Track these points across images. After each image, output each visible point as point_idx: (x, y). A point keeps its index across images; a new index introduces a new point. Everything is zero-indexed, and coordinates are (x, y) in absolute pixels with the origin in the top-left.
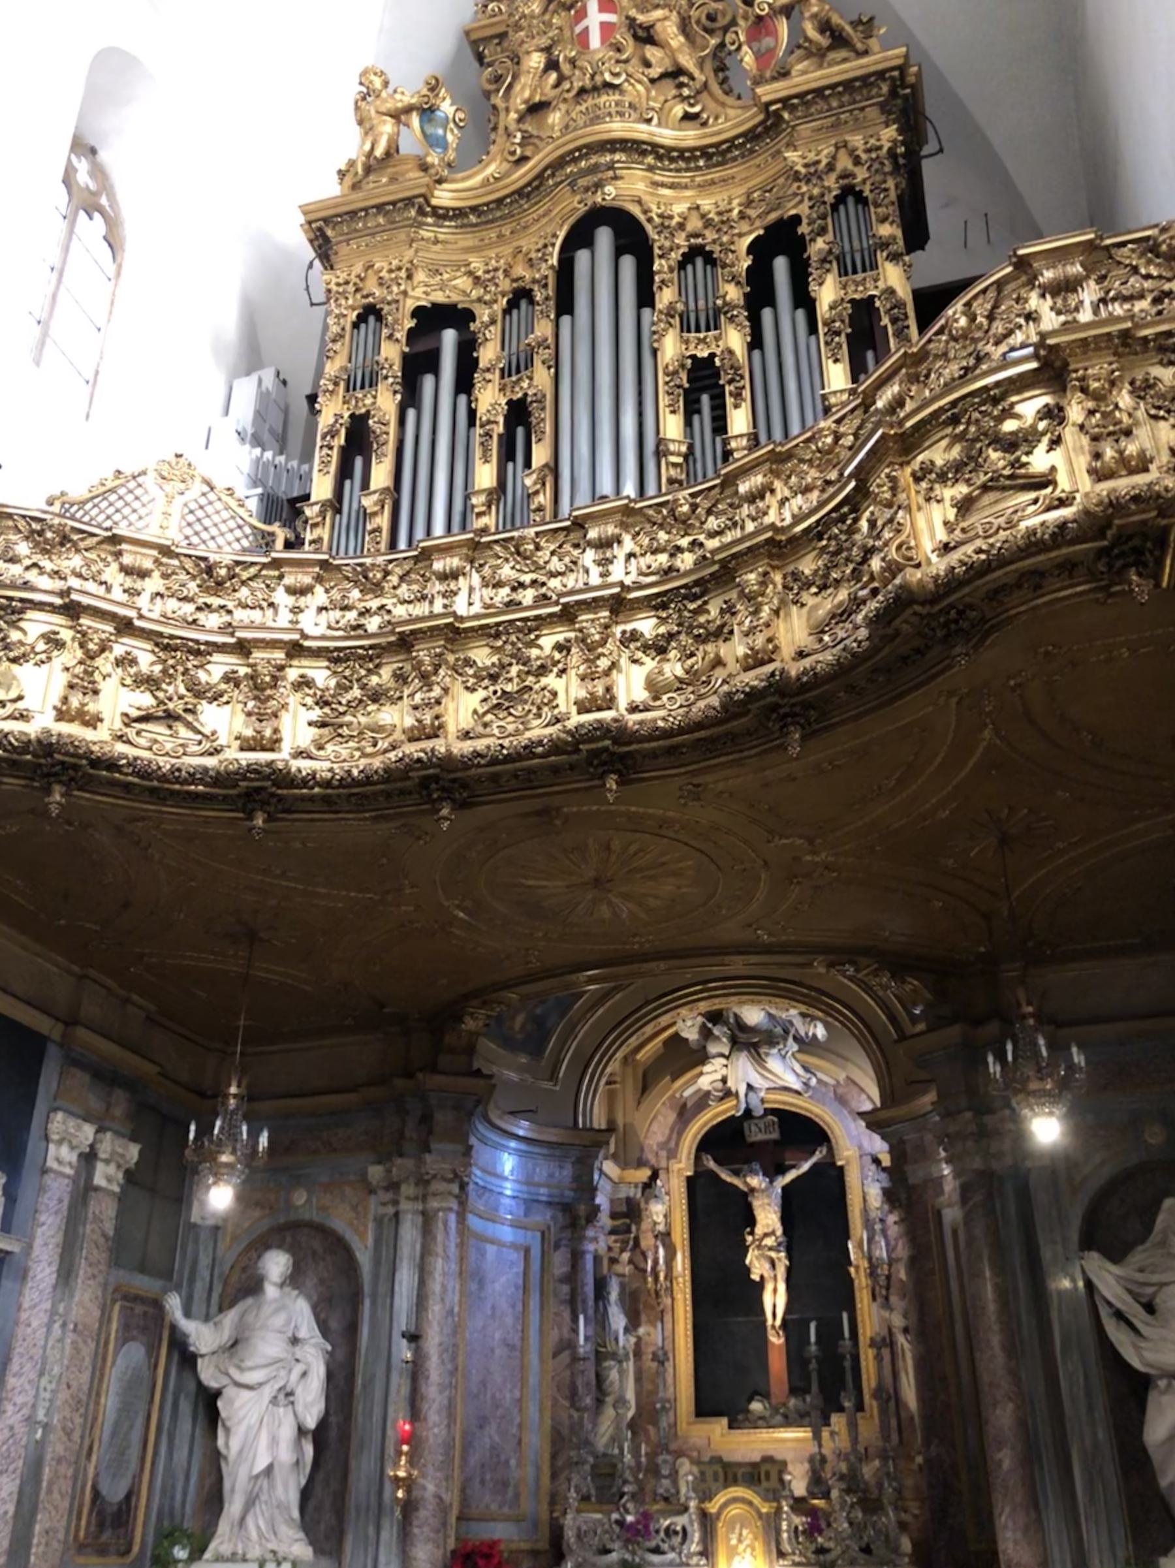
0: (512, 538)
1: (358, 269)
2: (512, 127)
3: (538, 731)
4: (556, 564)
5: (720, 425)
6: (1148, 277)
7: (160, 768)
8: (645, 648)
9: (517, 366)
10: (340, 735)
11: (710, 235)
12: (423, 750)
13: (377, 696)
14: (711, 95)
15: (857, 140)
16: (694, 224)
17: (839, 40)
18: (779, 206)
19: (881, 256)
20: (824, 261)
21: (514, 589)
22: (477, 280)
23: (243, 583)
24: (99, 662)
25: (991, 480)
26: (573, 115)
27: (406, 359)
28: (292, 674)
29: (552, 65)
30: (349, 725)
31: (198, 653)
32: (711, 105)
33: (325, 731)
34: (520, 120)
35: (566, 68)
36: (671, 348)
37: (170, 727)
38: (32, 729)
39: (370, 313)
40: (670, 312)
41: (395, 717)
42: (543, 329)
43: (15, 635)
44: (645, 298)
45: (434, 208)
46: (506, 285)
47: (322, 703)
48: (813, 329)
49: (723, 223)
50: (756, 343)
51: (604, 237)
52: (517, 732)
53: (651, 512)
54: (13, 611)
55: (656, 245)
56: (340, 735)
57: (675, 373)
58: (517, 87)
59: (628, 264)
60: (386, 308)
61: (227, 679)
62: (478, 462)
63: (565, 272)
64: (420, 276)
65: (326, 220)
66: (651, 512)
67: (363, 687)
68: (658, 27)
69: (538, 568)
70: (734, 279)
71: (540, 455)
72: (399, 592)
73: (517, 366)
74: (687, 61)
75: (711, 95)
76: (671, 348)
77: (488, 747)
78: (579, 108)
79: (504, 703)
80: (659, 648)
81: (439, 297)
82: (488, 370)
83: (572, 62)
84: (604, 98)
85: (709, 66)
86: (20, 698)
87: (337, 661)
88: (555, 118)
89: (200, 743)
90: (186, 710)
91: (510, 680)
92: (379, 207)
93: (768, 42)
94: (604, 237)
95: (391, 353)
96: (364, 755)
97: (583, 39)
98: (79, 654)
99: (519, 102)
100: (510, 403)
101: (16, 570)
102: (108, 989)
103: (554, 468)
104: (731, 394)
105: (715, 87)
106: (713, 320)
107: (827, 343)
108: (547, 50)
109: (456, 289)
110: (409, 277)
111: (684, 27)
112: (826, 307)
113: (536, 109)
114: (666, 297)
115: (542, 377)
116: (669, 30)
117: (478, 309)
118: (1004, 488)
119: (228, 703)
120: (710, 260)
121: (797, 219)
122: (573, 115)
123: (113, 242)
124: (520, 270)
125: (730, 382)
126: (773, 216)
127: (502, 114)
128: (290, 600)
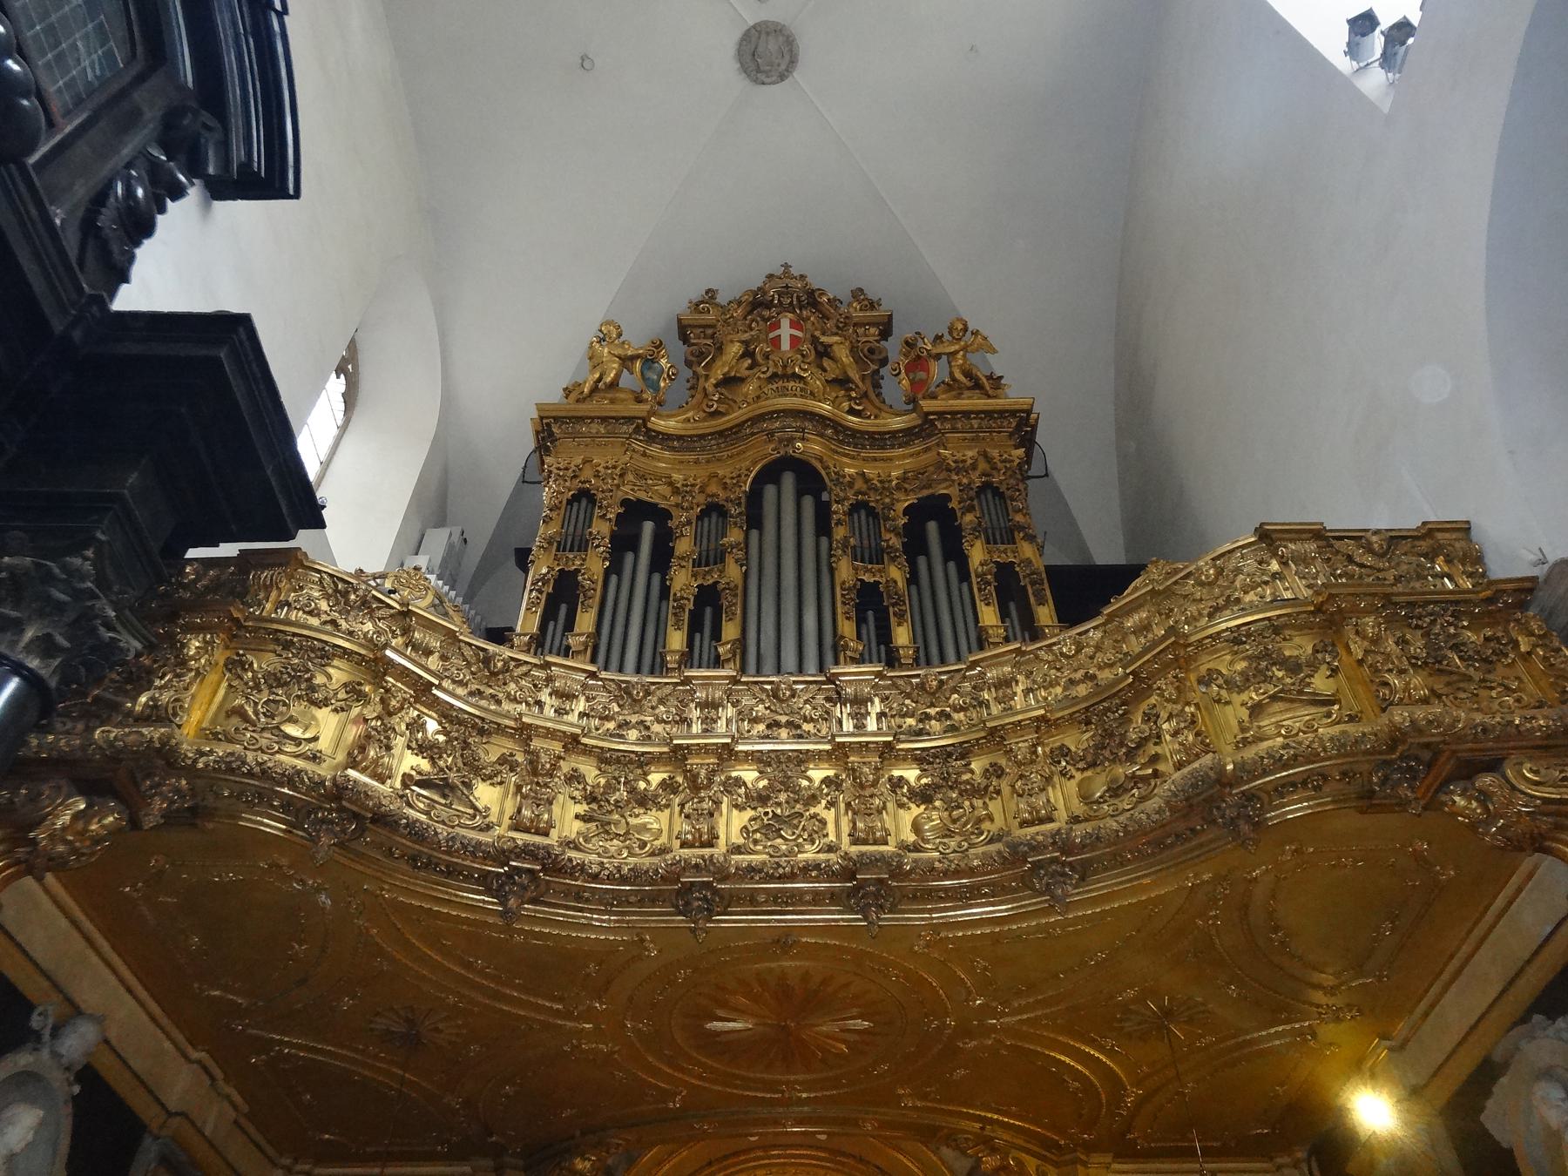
1: (578, 460)
2: (710, 389)
3: (809, 854)
5: (885, 636)
6: (1362, 566)
7: (436, 833)
10: (607, 832)
11: (873, 497)
12: (702, 857)
13: (644, 801)
14: (871, 402)
15: (995, 453)
16: (859, 484)
17: (977, 386)
18: (930, 486)
19: (1019, 536)
20: (974, 529)
21: (769, 727)
22: (676, 491)
23: (513, 679)
24: (395, 720)
25: (1281, 691)
27: (614, 537)
28: (565, 767)
29: (748, 354)
30: (616, 824)
31: (482, 732)
32: (870, 407)
33: (592, 825)
34: (716, 386)
35: (759, 358)
37: (444, 796)
38: (324, 771)
39: (585, 496)
40: (845, 544)
41: (658, 823)
42: (734, 536)
43: (319, 679)
45: (649, 430)
46: (701, 498)
47: (591, 798)
48: (964, 575)
49: (884, 487)
50: (913, 579)
51: (788, 480)
52: (790, 853)
54: (325, 654)
56: (607, 832)
57: (849, 589)
58: (719, 363)
60: (600, 496)
61: (503, 760)
62: (670, 629)
63: (754, 499)
64: (630, 477)
65: (556, 419)
66: (901, 682)
67: (632, 790)
68: (835, 348)
70: (894, 530)
71: (730, 631)
73: (711, 558)
74: (854, 375)
75: (871, 402)
77: (764, 863)
79: (771, 829)
80: (923, 796)
81: (643, 496)
82: (683, 558)
83: (767, 357)
85: (868, 382)
86: (315, 739)
87: (607, 762)
88: (750, 388)
89: (474, 817)
91: (779, 804)
92: (604, 419)
93: (922, 375)
94: (788, 480)
95: (601, 530)
96: (631, 854)
97: (776, 342)
98: (379, 708)
99: (718, 373)
101: (315, 622)
102: (213, 1078)
103: (742, 642)
104: (895, 614)
105: (872, 396)
106: (876, 555)
107: (980, 590)
108: (746, 343)
109: (658, 494)
110: (621, 476)
111: (853, 350)
113: (729, 381)
114: (840, 533)
115: (733, 572)
116: (843, 353)
117: (674, 512)
118: (1292, 701)
119: (501, 783)
120: (872, 512)
121: (947, 498)
123: (350, 398)
124: (713, 488)
125: (894, 605)
126: (925, 493)
127: (702, 380)
128: (555, 702)
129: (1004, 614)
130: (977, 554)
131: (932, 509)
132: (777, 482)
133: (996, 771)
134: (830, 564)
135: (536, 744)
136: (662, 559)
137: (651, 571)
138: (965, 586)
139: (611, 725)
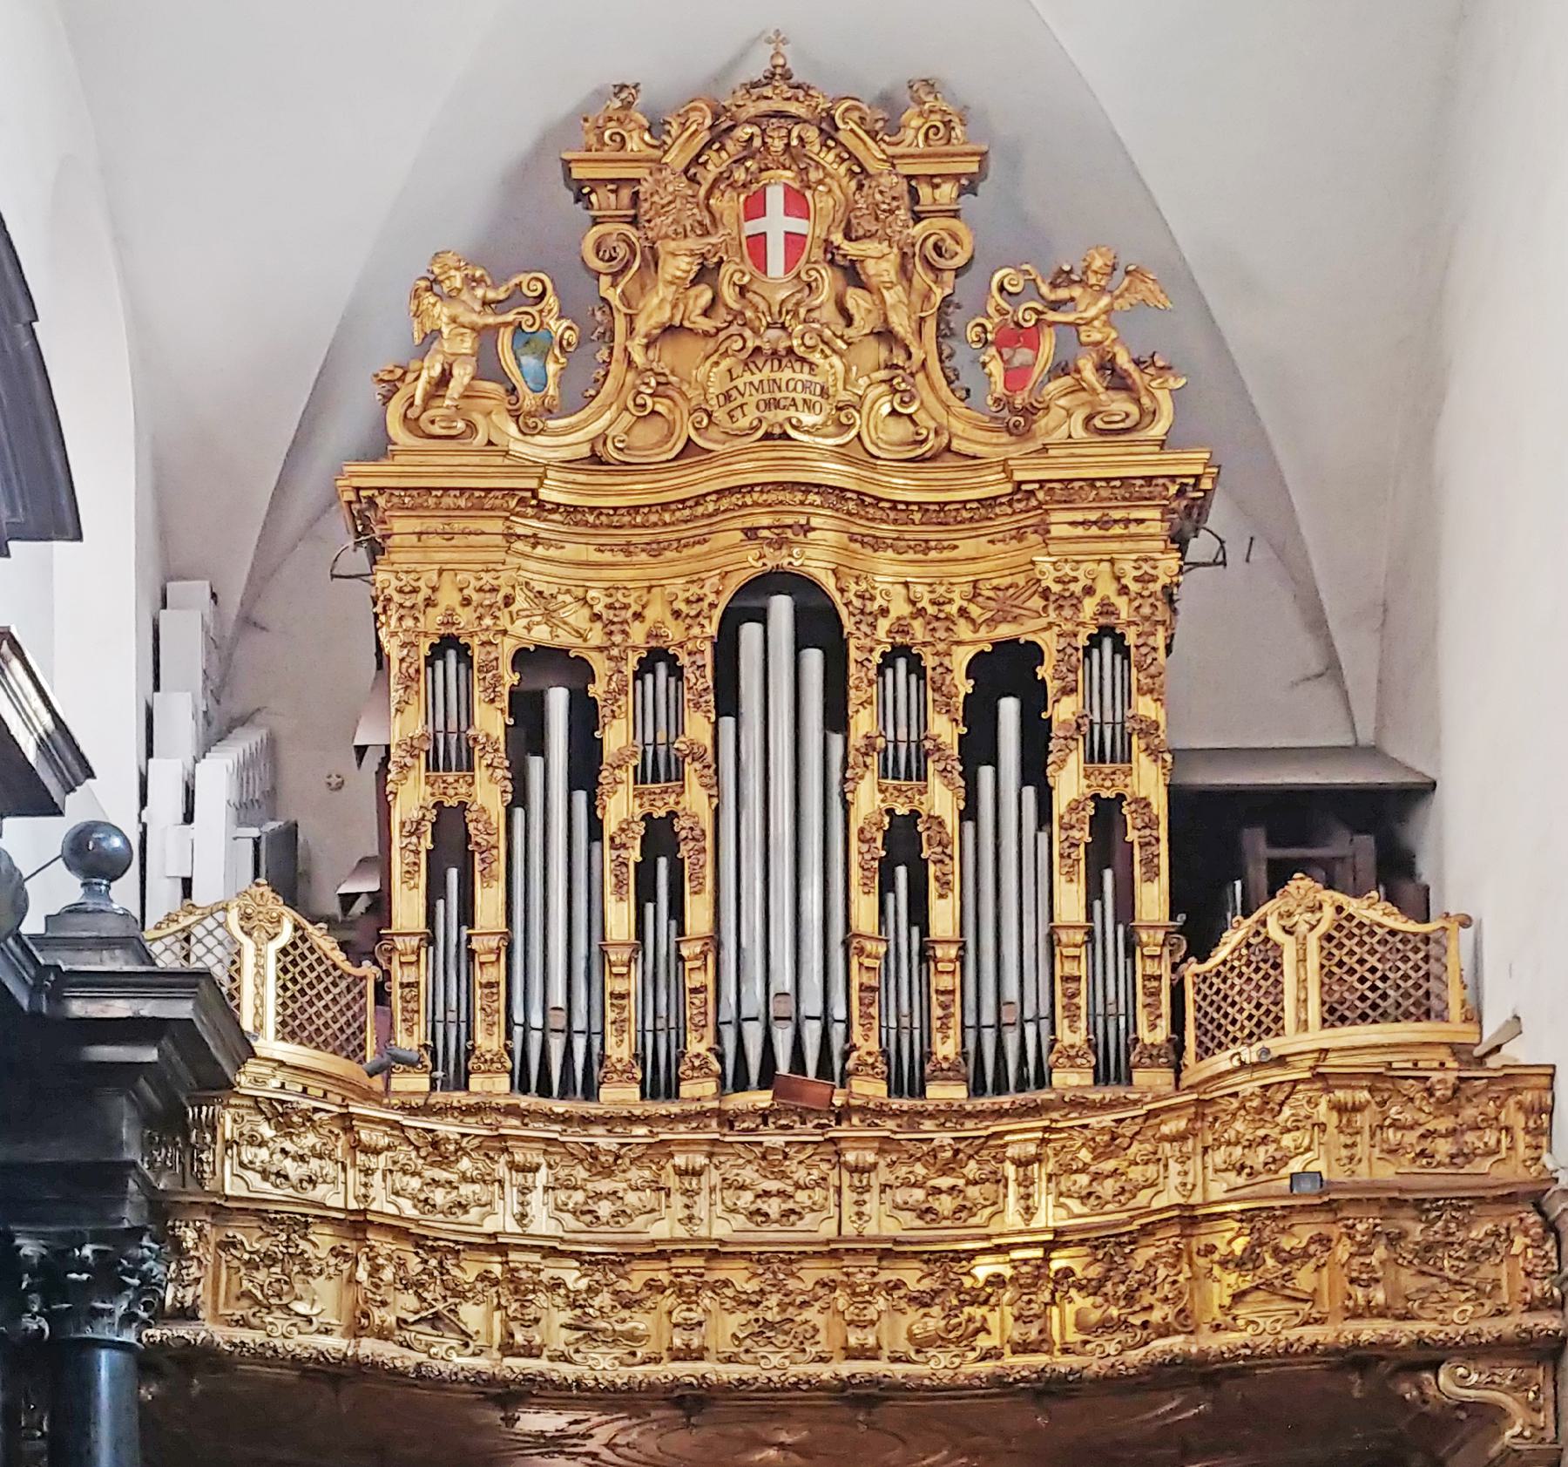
0: (761, 1143)
4: (801, 1175)
5: (919, 913)
8: (912, 1300)
9: (659, 769)
26: (739, 383)
36: (868, 799)
37: (434, 1328)
42: (698, 727)
44: (836, 718)
48: (1044, 815)
50: (970, 812)
51: (781, 608)
53: (910, 1146)
55: (852, 643)
59: (814, 659)
69: (783, 1175)
72: (628, 1175)
73: (659, 769)
76: (869, 799)
78: (748, 377)
80: (921, 1301)
84: (787, 374)
90: (450, 1311)
94: (781, 608)
95: (491, 721)
100: (647, 817)
109: (571, 629)
112: (1063, 809)
114: (863, 723)
122: (739, 383)
128: (518, 1178)
129: (1094, 891)
130: (1070, 782)
131: (1009, 668)
132: (762, 616)
133: (997, 1281)
134: (843, 794)
135: (513, 1256)
136: (586, 768)
137: (572, 787)
138: (1043, 837)
139: (579, 1196)
